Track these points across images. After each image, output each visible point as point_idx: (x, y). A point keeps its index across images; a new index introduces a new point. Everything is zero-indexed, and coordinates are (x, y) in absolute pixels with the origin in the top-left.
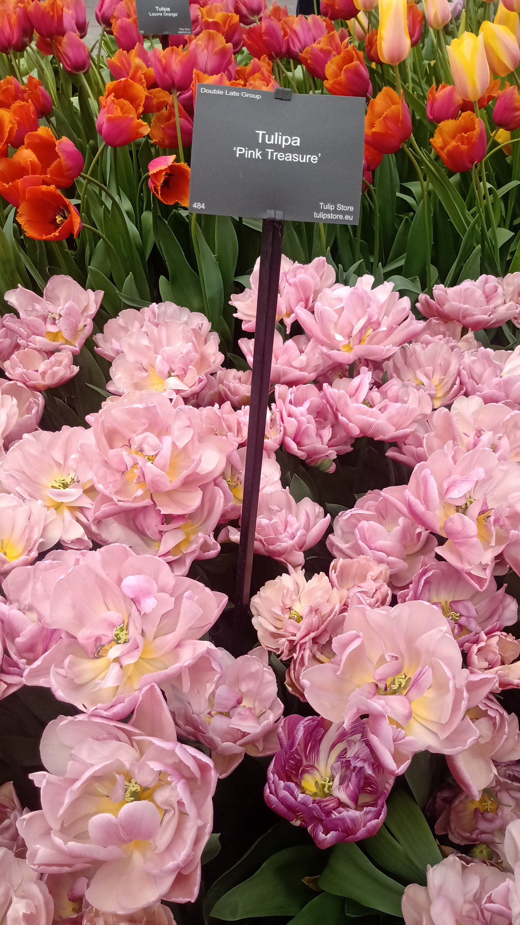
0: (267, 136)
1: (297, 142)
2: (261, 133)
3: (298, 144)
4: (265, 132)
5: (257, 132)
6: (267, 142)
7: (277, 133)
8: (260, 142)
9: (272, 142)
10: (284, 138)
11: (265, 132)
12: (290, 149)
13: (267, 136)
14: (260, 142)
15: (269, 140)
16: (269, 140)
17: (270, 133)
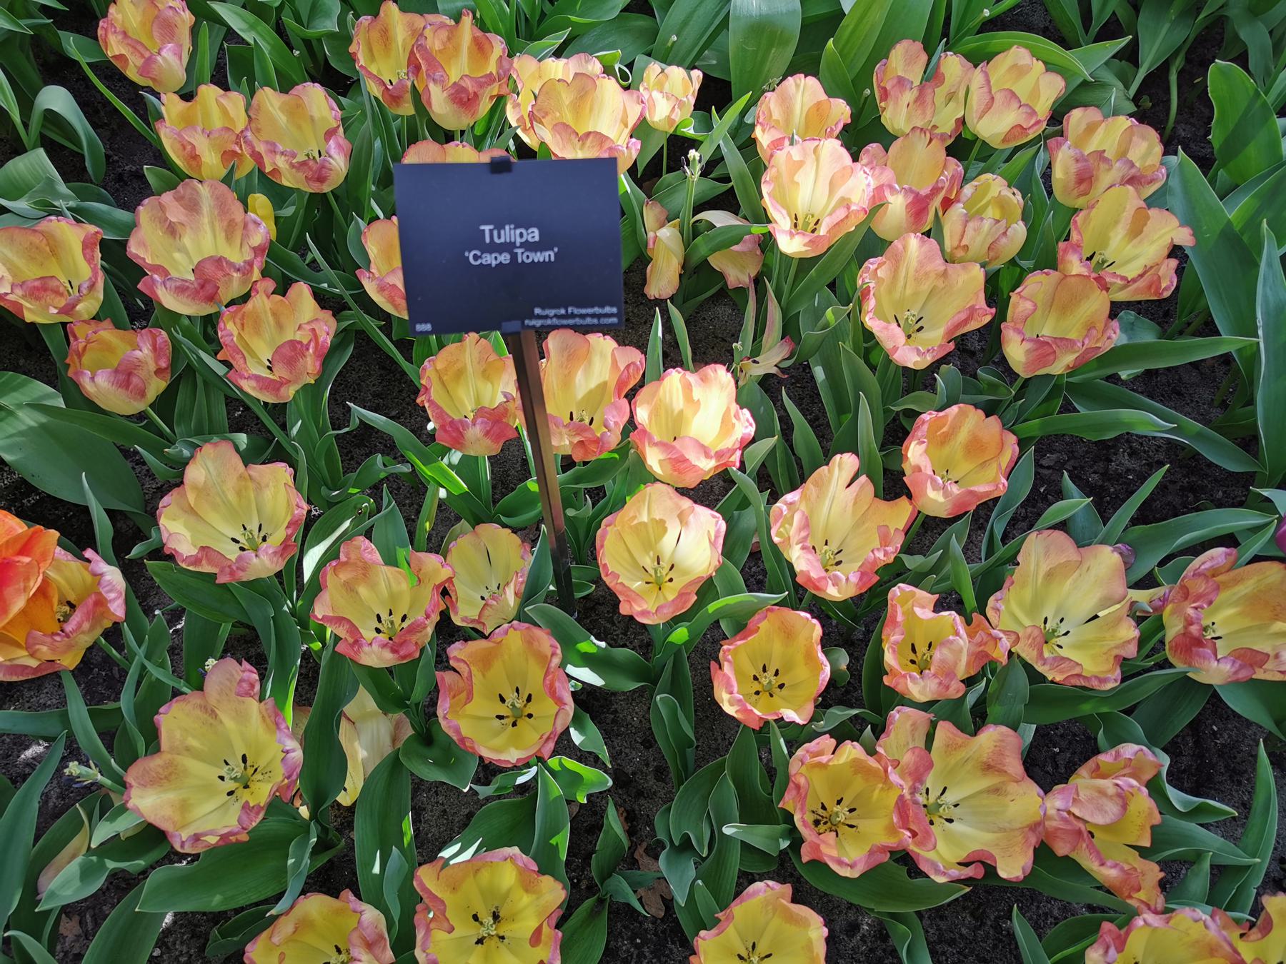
0: (495, 233)
1: (534, 235)
2: (487, 228)
3: (537, 239)
4: (491, 227)
5: (482, 227)
6: (496, 240)
7: (507, 227)
8: (488, 240)
9: (502, 240)
10: (518, 231)
11: (491, 227)
12: (528, 246)
13: (495, 233)
14: (488, 240)
15: (499, 237)
16: (499, 237)
17: (500, 227)
